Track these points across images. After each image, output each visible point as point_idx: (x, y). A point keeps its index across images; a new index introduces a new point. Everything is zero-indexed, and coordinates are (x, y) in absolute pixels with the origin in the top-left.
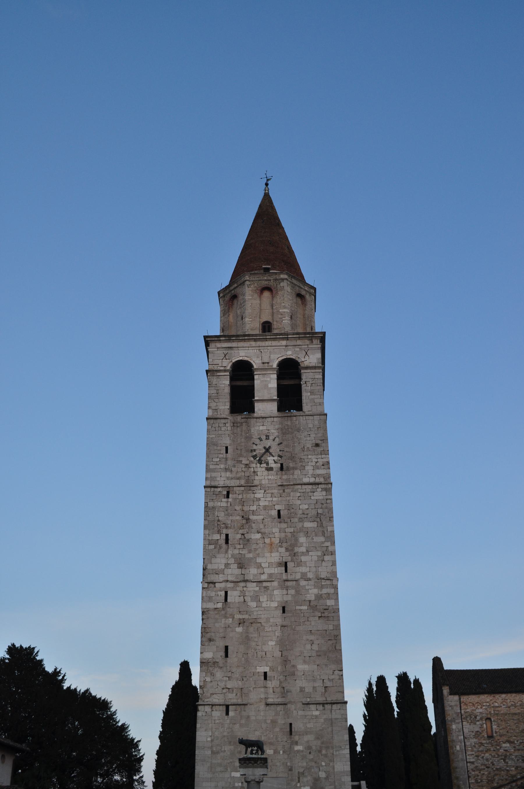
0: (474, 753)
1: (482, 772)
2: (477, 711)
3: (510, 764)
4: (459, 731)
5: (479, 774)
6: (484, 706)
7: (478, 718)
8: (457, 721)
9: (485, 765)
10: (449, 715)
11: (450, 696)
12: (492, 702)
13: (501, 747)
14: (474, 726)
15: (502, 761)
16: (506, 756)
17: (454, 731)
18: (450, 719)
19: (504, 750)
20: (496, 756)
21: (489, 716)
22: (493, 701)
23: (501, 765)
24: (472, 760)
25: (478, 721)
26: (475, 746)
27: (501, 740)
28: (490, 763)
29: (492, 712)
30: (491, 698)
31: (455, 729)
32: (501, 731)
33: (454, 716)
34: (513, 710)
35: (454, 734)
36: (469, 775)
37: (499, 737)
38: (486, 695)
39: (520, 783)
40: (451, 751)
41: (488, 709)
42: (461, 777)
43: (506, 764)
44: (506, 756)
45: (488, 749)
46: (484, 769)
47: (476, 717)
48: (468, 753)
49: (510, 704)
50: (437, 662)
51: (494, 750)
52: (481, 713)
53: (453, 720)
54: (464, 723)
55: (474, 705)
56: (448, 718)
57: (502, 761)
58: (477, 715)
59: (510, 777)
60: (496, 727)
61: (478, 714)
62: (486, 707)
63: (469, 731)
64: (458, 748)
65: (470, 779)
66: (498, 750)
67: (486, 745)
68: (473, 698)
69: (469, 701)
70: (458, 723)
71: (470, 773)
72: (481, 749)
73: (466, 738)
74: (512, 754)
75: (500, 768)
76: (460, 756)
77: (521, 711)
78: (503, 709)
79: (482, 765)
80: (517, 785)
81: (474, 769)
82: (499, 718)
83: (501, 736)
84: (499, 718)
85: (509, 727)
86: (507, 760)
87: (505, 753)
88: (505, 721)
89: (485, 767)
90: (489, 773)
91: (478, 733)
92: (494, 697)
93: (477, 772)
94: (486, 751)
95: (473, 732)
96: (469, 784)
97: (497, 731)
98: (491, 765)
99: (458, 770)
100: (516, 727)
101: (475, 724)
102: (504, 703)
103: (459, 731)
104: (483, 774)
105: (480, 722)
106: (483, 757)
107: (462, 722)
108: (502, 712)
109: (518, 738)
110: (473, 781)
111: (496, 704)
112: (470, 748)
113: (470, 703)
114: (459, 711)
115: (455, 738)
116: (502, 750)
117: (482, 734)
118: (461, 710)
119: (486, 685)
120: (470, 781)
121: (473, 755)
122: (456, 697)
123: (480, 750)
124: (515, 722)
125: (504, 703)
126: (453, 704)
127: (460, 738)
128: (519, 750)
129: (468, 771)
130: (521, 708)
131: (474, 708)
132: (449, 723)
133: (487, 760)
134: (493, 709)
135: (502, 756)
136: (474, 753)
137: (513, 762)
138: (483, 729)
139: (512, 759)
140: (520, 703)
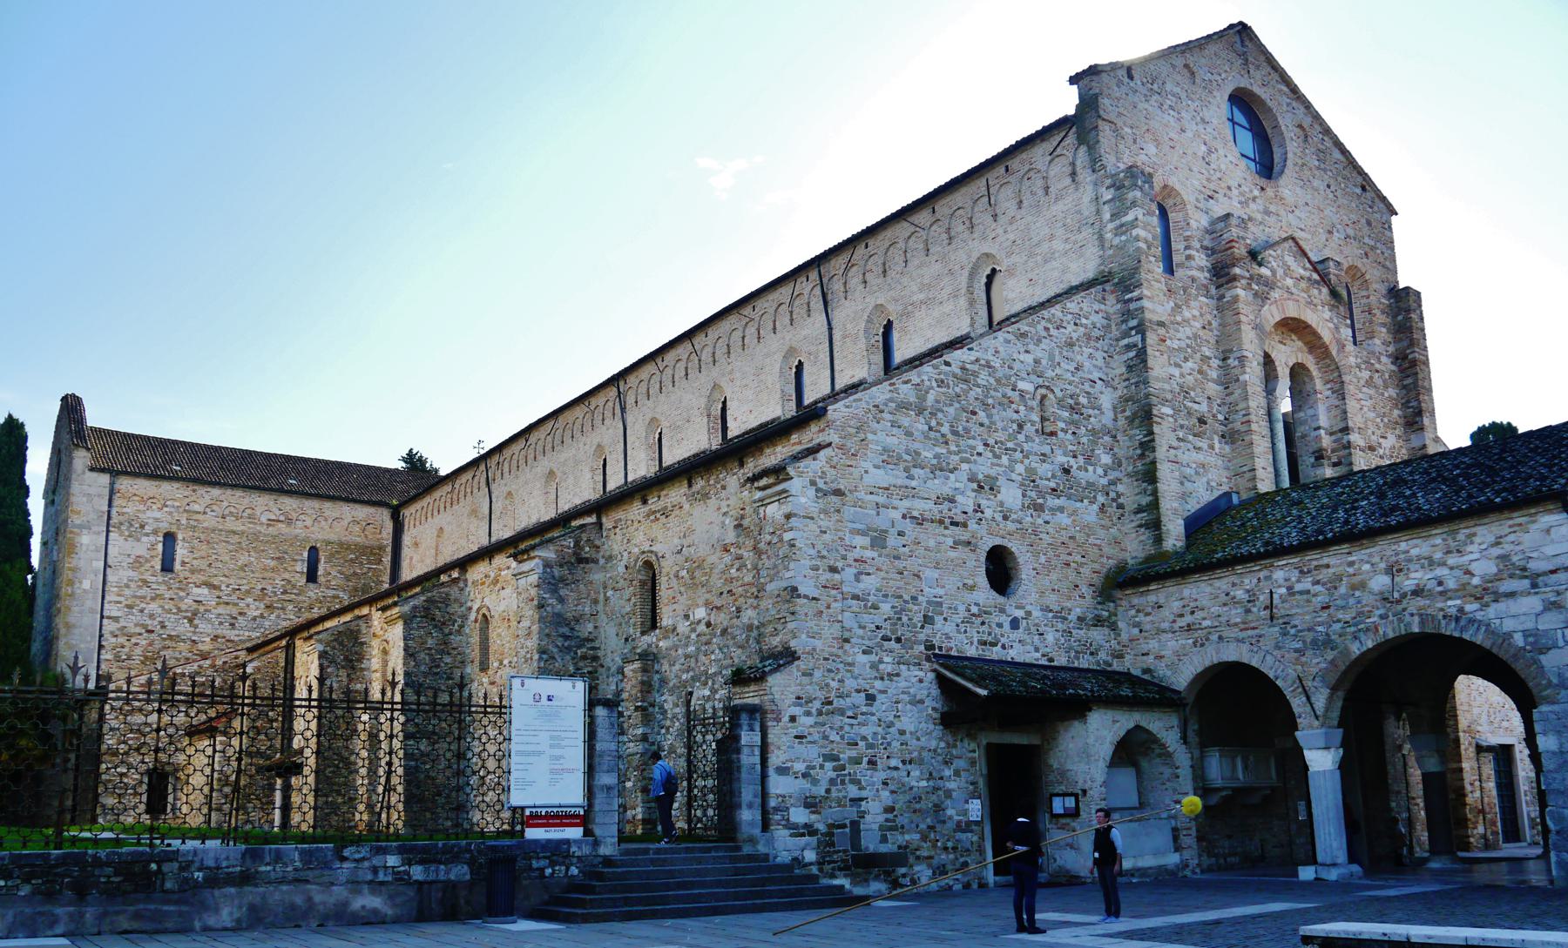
0: (122, 599)
1: (134, 640)
2: (149, 514)
3: (202, 630)
4: (97, 551)
5: (127, 644)
6: (167, 506)
7: (148, 529)
8: (95, 529)
9: (144, 626)
10: (79, 513)
11: (89, 474)
12: (187, 500)
13: (188, 594)
14: (135, 544)
15: (186, 621)
16: (195, 614)
17: (84, 548)
18: (78, 522)
19: (195, 601)
20: (175, 611)
21: (174, 529)
22: (192, 499)
23: (181, 629)
24: (114, 613)
25: (147, 535)
26: (127, 586)
27: (190, 581)
28: (156, 623)
29: (184, 521)
30: (186, 494)
31: (88, 545)
32: (195, 562)
33: (93, 516)
34: (231, 524)
35: (82, 555)
36: (103, 643)
37: (187, 574)
38: (176, 485)
39: (221, 663)
40: (65, 590)
41: (176, 514)
42: (82, 646)
43: (192, 629)
44: (195, 614)
45: (157, 595)
46: (140, 634)
47: (142, 527)
48: (108, 598)
49: (226, 512)
50: (71, 408)
51: (171, 599)
52: (156, 520)
53: (87, 526)
54: (111, 534)
55: (143, 501)
56: (75, 520)
57: (186, 621)
58: (147, 523)
59: (196, 655)
60: (185, 552)
61: (150, 521)
62: (172, 510)
63: (120, 554)
64: (86, 585)
65: (103, 652)
66: (182, 599)
67: (154, 586)
68: (144, 486)
69: (134, 491)
70: (99, 533)
71: (107, 640)
72: (141, 593)
73: (110, 567)
74: (209, 611)
75: (178, 636)
76: (89, 603)
77: (249, 528)
78: (209, 521)
79: (136, 625)
80: (213, 666)
81: (117, 633)
82: (196, 534)
83: (193, 572)
84: (196, 534)
85: (214, 557)
86: (196, 622)
87: (195, 606)
88: (208, 542)
89: (143, 631)
90: (150, 645)
91: (141, 560)
92: (194, 491)
93: (122, 640)
94: (153, 599)
95: (129, 555)
96: (99, 662)
97: (186, 560)
98: (159, 627)
99: (76, 631)
100: (231, 559)
101: (139, 540)
102: (214, 507)
103: (97, 551)
104: (137, 644)
105: (152, 538)
106: (142, 611)
107: (108, 531)
108: (205, 525)
109: (232, 581)
110: (109, 656)
111: (196, 507)
112: (116, 589)
113: (135, 495)
114: (106, 508)
115: (82, 564)
116: (189, 601)
117: (150, 562)
118: (110, 505)
119: (180, 466)
120: (102, 657)
121: (120, 602)
122: (105, 479)
123: (138, 594)
124: (231, 547)
125: (214, 507)
126: (92, 491)
127: (95, 564)
128: (227, 604)
129: (101, 636)
130: (250, 523)
131: (141, 507)
132: (75, 530)
133: (151, 616)
134: (185, 515)
135: (186, 611)
136: (122, 599)
137: (210, 626)
138: (154, 553)
139: (209, 621)
140: (249, 511)
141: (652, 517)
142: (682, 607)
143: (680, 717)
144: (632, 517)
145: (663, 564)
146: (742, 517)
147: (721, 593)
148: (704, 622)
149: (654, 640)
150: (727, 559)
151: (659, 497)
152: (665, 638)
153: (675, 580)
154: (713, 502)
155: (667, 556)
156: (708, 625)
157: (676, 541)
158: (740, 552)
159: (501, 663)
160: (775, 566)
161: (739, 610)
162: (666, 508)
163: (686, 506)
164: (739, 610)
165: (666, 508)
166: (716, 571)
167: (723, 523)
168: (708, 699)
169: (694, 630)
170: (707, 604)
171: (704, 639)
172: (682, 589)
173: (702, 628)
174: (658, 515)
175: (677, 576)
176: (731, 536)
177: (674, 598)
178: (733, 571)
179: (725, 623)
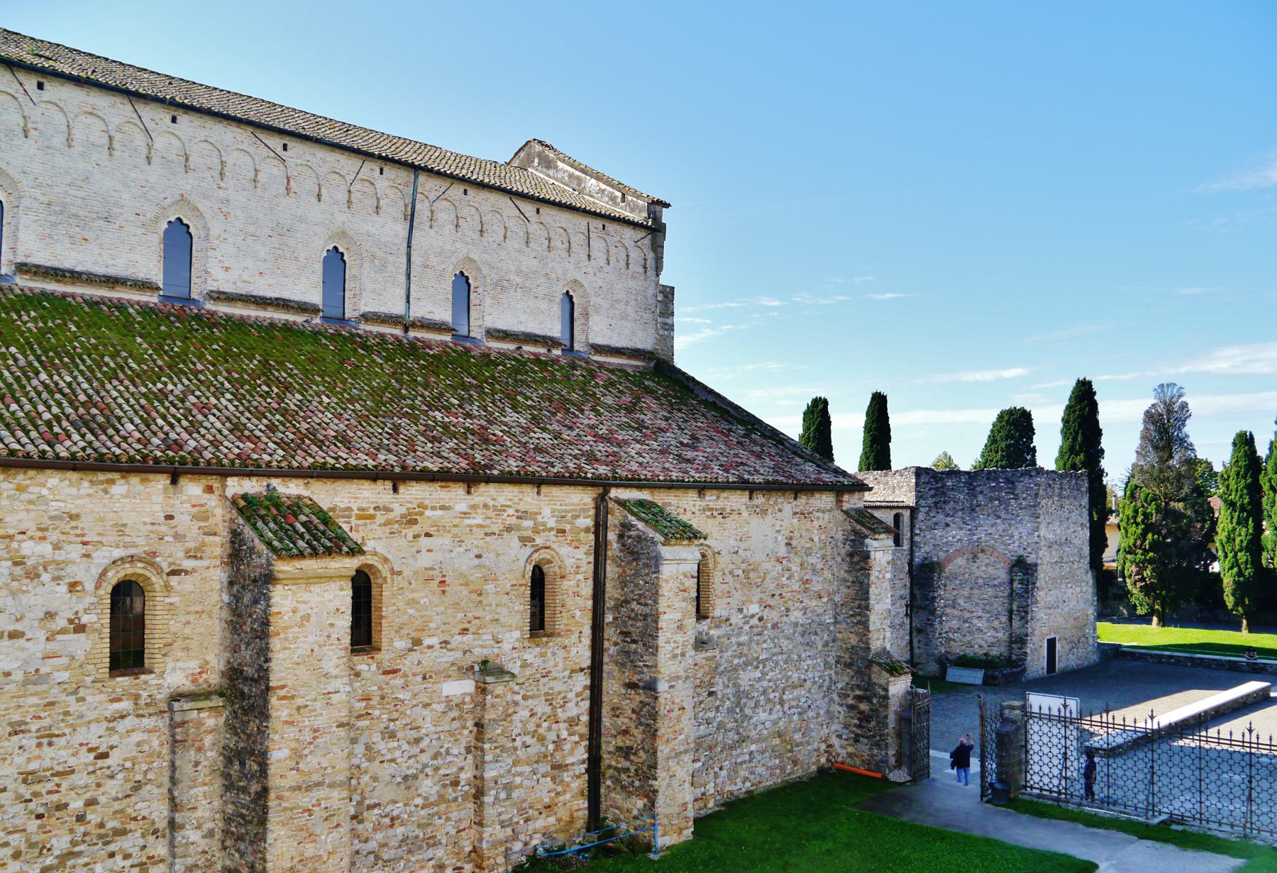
141: (709, 513)
142: (737, 602)
143: (730, 696)
144: (686, 506)
145: (718, 560)
146: (791, 538)
147: (773, 595)
148: (757, 617)
149: (706, 628)
150: (779, 567)
151: (718, 498)
152: (717, 627)
153: (730, 577)
154: (769, 518)
155: (723, 553)
156: (761, 619)
157: (732, 542)
158: (790, 565)
159: (417, 642)
160: (880, 594)
161: (788, 610)
162: (724, 509)
163: (745, 514)
164: (788, 610)
165: (724, 509)
166: (769, 576)
167: (776, 538)
168: (759, 680)
169: (747, 622)
170: (761, 601)
171: (755, 630)
172: (738, 586)
173: (755, 621)
174: (715, 513)
175: (731, 573)
176: (782, 551)
177: (729, 592)
178: (784, 579)
179: (776, 619)
